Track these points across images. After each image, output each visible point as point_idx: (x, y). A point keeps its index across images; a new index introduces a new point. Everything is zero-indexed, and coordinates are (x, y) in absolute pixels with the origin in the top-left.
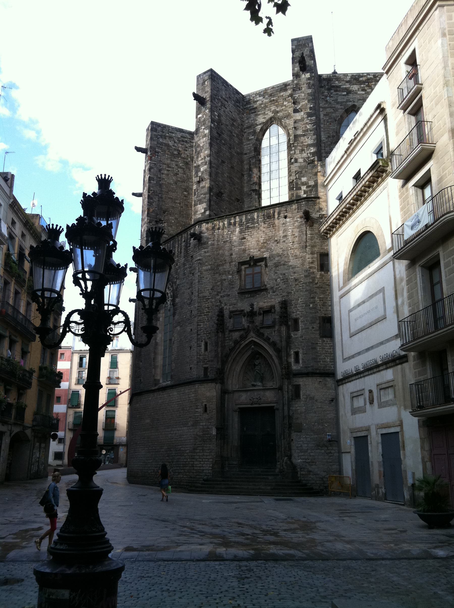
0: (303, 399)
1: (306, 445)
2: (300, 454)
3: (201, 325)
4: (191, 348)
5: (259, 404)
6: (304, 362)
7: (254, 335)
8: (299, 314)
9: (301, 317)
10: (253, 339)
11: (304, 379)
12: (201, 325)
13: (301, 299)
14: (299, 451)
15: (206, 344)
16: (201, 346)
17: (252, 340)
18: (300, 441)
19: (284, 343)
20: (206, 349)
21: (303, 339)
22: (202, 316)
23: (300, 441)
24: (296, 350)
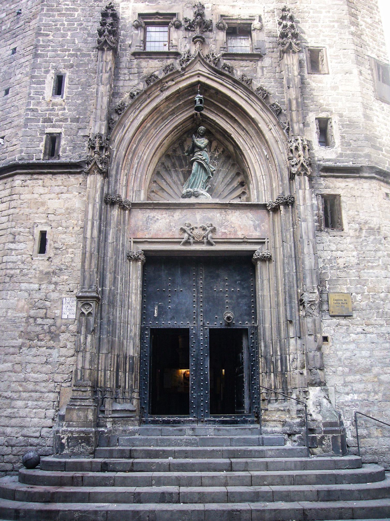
0: (352, 233)
1: (365, 353)
2: (350, 378)
3: (48, 35)
4: (7, 92)
5: (209, 243)
6: (346, 144)
7: (204, 70)
8: (324, 41)
9: (330, 46)
10: (202, 79)
11: (351, 183)
12: (48, 35)
13: (326, 12)
14: (347, 370)
15: (60, 80)
16: (44, 82)
17: (199, 82)
18: (350, 342)
19: (293, 93)
20: (58, 90)
21: (338, 94)
22: (53, 16)
23: (350, 342)
24: (323, 115)
